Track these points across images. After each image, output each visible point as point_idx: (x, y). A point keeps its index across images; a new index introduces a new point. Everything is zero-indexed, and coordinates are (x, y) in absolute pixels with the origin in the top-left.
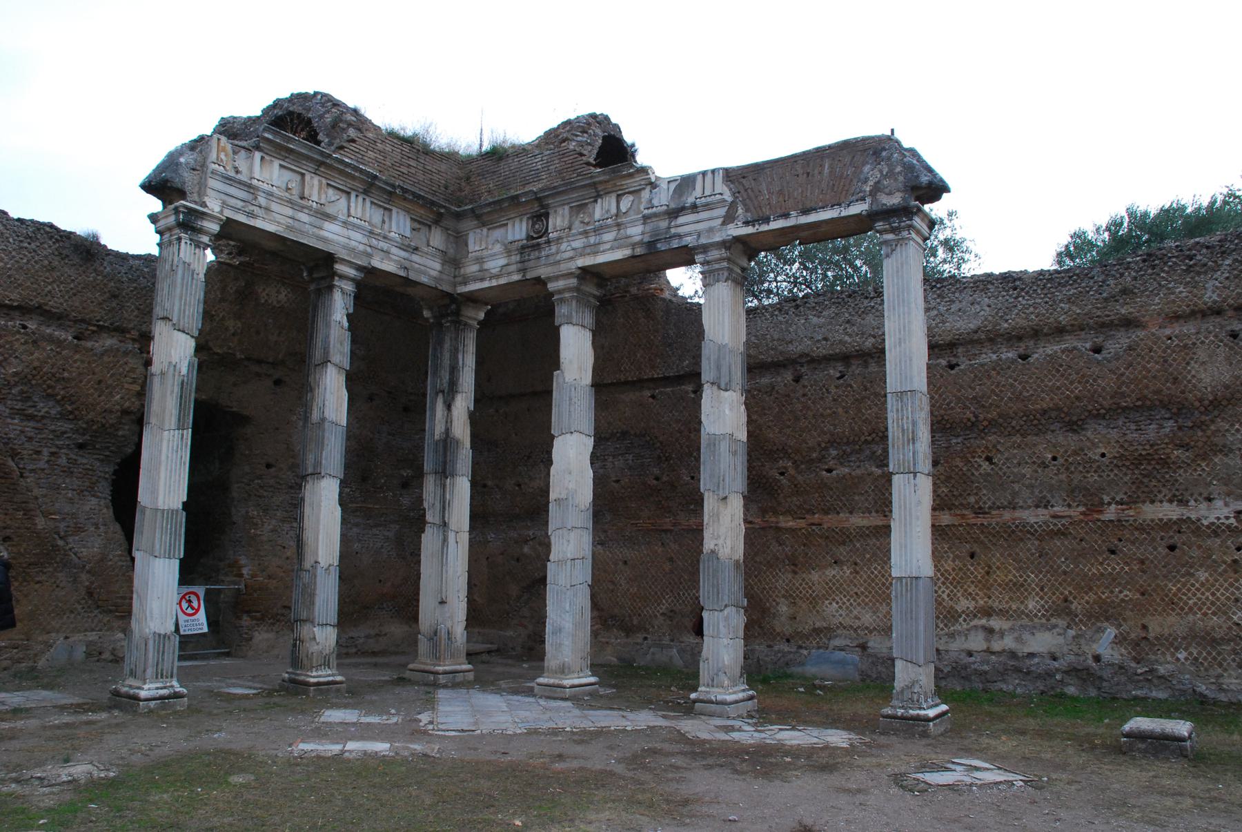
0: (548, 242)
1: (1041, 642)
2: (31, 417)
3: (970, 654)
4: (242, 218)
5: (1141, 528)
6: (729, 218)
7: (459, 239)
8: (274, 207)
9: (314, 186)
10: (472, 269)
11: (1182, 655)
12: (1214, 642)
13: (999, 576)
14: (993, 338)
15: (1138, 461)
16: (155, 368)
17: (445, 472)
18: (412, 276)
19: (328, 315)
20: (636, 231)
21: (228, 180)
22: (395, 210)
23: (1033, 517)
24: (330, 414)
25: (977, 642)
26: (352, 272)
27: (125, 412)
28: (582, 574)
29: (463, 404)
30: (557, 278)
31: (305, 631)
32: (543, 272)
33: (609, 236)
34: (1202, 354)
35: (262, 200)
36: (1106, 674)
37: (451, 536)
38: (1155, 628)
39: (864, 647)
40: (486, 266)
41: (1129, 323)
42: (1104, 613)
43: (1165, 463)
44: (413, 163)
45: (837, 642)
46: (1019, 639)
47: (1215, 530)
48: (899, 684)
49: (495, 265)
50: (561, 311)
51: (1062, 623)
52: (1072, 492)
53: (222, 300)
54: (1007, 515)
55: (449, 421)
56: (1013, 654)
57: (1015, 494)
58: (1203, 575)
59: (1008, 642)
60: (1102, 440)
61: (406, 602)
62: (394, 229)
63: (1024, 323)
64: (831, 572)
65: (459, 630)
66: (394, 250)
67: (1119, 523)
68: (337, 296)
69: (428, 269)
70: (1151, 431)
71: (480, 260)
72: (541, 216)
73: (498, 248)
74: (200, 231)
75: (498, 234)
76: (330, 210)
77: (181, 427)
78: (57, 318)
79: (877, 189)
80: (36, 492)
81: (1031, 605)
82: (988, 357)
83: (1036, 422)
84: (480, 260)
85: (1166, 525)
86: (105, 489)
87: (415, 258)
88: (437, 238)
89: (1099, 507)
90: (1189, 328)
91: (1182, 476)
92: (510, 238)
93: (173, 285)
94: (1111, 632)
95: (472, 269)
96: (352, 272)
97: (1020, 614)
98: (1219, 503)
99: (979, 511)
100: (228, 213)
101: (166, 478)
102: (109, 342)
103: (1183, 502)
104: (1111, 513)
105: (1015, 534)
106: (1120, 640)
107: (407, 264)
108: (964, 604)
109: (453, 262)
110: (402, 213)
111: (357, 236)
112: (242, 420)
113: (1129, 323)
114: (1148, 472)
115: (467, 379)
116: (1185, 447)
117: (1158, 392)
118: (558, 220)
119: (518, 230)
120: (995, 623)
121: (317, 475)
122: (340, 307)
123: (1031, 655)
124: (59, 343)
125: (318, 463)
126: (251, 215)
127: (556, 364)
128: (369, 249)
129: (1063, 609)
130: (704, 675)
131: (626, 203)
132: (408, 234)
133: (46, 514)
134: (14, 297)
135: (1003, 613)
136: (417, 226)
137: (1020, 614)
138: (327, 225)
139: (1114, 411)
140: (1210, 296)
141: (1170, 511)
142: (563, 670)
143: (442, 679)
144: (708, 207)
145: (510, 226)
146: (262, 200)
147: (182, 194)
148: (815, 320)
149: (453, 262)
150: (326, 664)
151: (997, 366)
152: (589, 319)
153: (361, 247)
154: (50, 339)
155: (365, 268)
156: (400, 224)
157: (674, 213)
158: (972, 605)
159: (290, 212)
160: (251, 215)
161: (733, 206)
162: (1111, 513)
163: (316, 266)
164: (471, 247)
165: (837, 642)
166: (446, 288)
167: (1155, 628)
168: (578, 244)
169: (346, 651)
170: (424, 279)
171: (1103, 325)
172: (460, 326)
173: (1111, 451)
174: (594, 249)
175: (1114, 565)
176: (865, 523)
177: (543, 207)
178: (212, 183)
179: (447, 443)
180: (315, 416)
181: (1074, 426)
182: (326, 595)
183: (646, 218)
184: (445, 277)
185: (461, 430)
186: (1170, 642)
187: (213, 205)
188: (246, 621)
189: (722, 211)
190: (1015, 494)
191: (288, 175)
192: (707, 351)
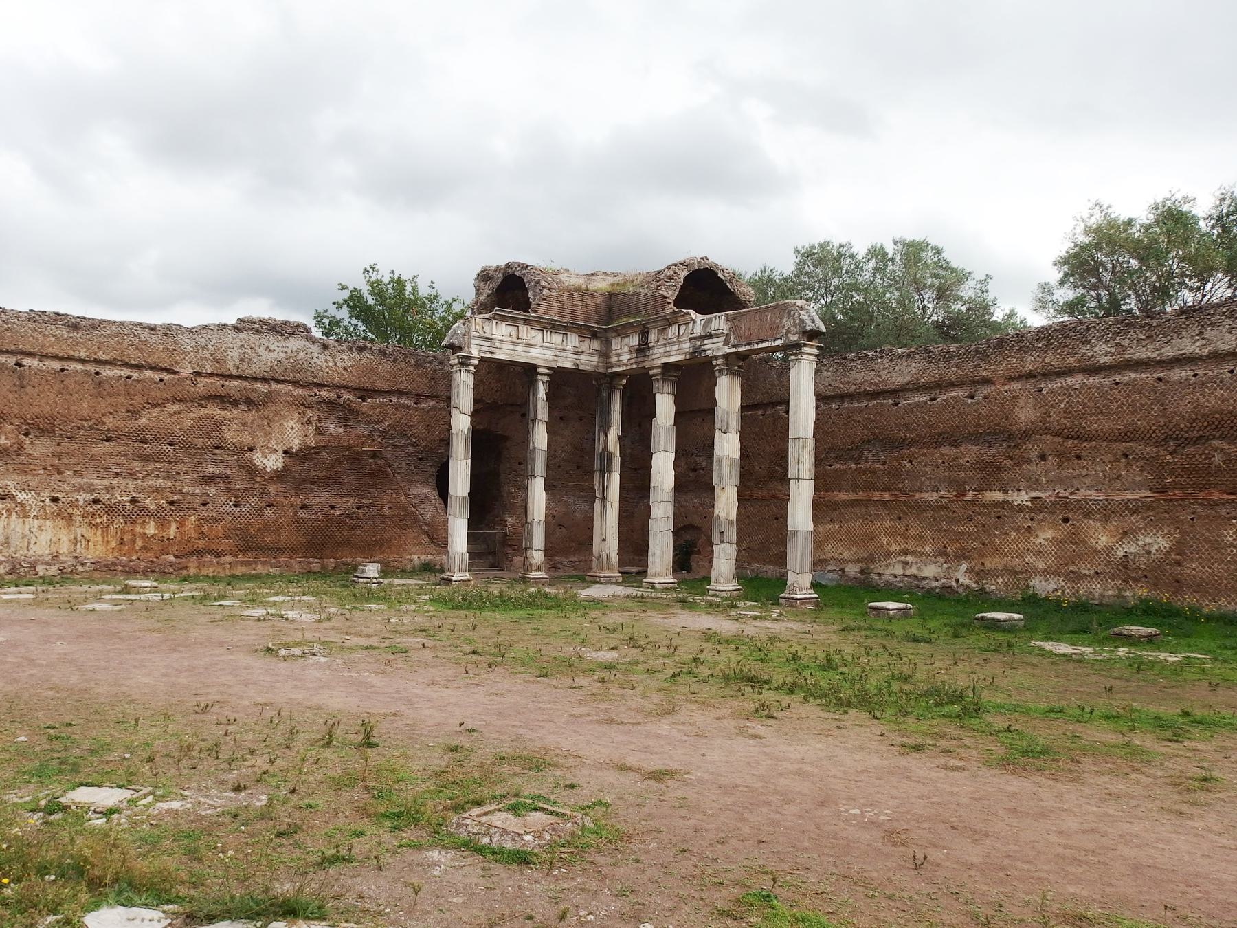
1: (930, 571)
2: (396, 446)
3: (895, 576)
4: (488, 355)
5: (984, 506)
6: (726, 343)
7: (608, 343)
8: (504, 346)
9: (524, 331)
10: (614, 359)
11: (1000, 581)
12: (1017, 573)
13: (912, 532)
14: (914, 387)
15: (986, 465)
16: (453, 431)
17: (604, 471)
18: (581, 367)
19: (535, 395)
20: (687, 346)
21: (482, 338)
23: (930, 497)
24: (538, 445)
25: (899, 570)
26: (546, 371)
27: (442, 440)
28: (669, 525)
29: (614, 433)
30: (652, 368)
31: (529, 553)
32: (648, 365)
33: (675, 348)
34: (1022, 404)
35: (497, 344)
36: (960, 590)
37: (608, 505)
38: (988, 565)
39: (843, 570)
41: (986, 381)
42: (962, 556)
43: (998, 467)
45: (830, 568)
46: (919, 569)
47: (1020, 508)
48: (789, 583)
49: (625, 358)
50: (656, 385)
51: (942, 560)
52: (950, 484)
53: (490, 372)
54: (917, 496)
55: (606, 442)
56: (916, 577)
57: (922, 483)
58: (1013, 534)
59: (914, 571)
60: (969, 453)
61: (585, 542)
63: (932, 379)
64: (829, 526)
65: (614, 557)
67: (972, 502)
68: (540, 384)
69: (589, 362)
70: (995, 450)
71: (618, 355)
72: (644, 333)
73: (626, 349)
74: (470, 365)
75: (626, 340)
76: (532, 342)
77: (466, 458)
78: (407, 394)
79: (788, 332)
80: (402, 484)
81: (927, 549)
82: (915, 399)
83: (939, 440)
84: (618, 355)
85: (997, 504)
86: (433, 480)
87: (582, 357)
88: (595, 345)
89: (962, 493)
90: (1015, 386)
91: (1007, 475)
93: (459, 393)
94: (964, 566)
95: (614, 359)
96: (546, 371)
97: (921, 554)
98: (1023, 492)
99: (904, 493)
100: (483, 354)
101: (460, 481)
102: (432, 403)
103: (1005, 492)
104: (969, 496)
105: (922, 507)
106: (970, 571)
108: (895, 547)
109: (605, 354)
111: (549, 352)
112: (505, 438)
113: (986, 381)
114: (990, 473)
115: (617, 419)
116: (1011, 458)
117: (998, 424)
118: (652, 337)
119: (634, 340)
120: (910, 558)
121: (533, 476)
122: (542, 390)
123: (925, 578)
124: (408, 407)
125: (533, 470)
126: (491, 353)
127: (653, 415)
129: (942, 553)
130: (713, 579)
131: (683, 328)
133: (406, 495)
134: (385, 386)
135: (914, 553)
137: (921, 554)
138: (532, 350)
139: (974, 437)
140: (1029, 367)
141: (998, 496)
142: (655, 575)
143: (602, 580)
144: (717, 336)
146: (497, 344)
147: (460, 349)
148: (825, 373)
149: (605, 354)
150: (539, 569)
151: (917, 405)
152: (672, 389)
154: (404, 406)
156: (573, 340)
157: (703, 338)
158: (898, 548)
159: (512, 347)
160: (491, 353)
161: (728, 336)
162: (969, 496)
163: (530, 370)
164: (614, 347)
165: (830, 568)
166: (601, 370)
167: (988, 565)
168: (661, 350)
169: (552, 566)
170: (588, 368)
171: (974, 382)
172: (612, 388)
173: (972, 459)
174: (668, 354)
175: (970, 528)
176: (846, 498)
178: (473, 341)
179: (606, 456)
180: (531, 446)
181: (956, 444)
182: (539, 538)
183: (691, 339)
185: (614, 445)
186: (993, 574)
187: (475, 353)
188: (510, 551)
189: (722, 339)
190: (922, 483)
191: (510, 328)
192: (718, 411)
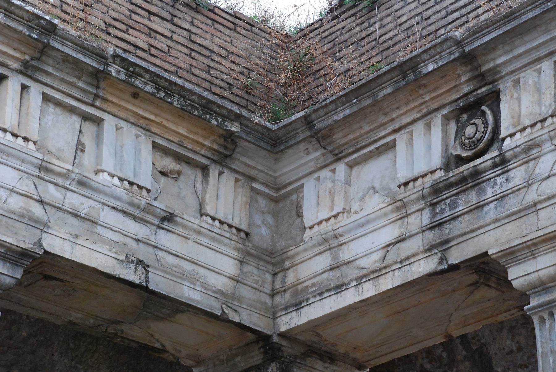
0: (502, 162)
7: (282, 200)
10: (311, 267)
18: (159, 283)
22: (110, 122)
30: (531, 248)
32: (492, 241)
40: (346, 254)
44: (158, 25)
49: (365, 249)
62: (108, 163)
66: (109, 217)
69: (200, 267)
71: (331, 243)
72: (480, 103)
73: (375, 203)
75: (375, 172)
87: (164, 239)
88: (225, 196)
92: (403, 175)
107: (144, 253)
109: (269, 258)
110: (130, 132)
119: (423, 150)
128: (37, 210)
132: (146, 180)
136: (169, 164)
145: (401, 146)
153: (16, 203)
155: (24, 254)
156: (123, 152)
170: (190, 294)
177: (481, 78)
184: (245, 292)
